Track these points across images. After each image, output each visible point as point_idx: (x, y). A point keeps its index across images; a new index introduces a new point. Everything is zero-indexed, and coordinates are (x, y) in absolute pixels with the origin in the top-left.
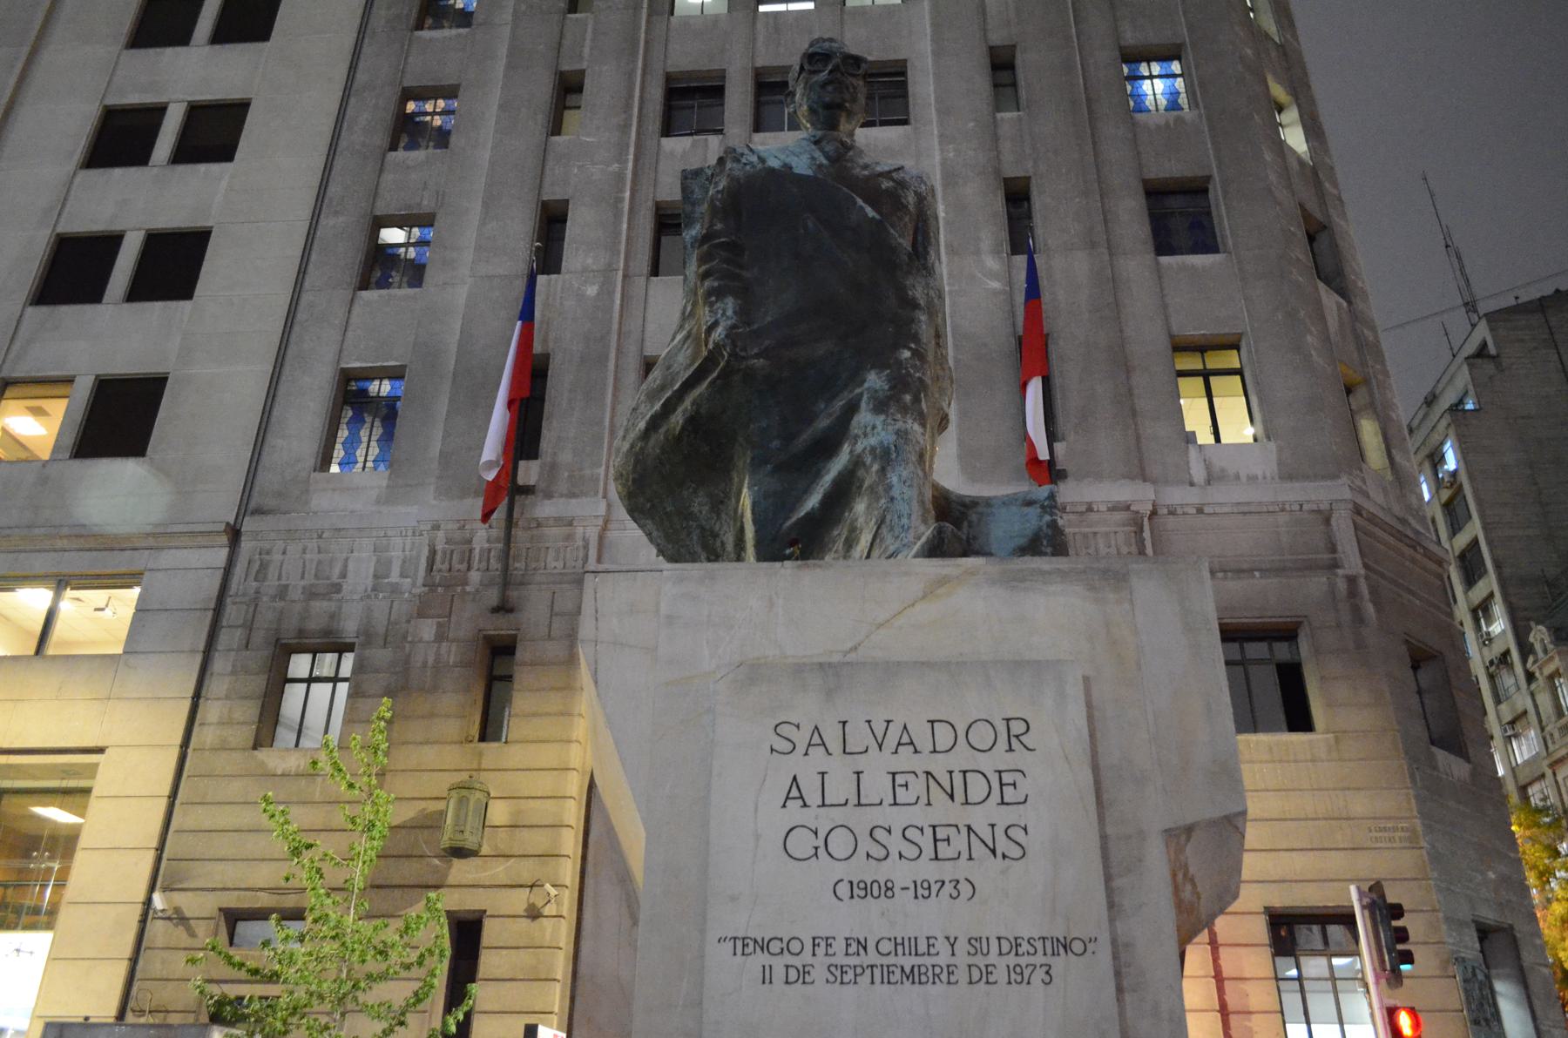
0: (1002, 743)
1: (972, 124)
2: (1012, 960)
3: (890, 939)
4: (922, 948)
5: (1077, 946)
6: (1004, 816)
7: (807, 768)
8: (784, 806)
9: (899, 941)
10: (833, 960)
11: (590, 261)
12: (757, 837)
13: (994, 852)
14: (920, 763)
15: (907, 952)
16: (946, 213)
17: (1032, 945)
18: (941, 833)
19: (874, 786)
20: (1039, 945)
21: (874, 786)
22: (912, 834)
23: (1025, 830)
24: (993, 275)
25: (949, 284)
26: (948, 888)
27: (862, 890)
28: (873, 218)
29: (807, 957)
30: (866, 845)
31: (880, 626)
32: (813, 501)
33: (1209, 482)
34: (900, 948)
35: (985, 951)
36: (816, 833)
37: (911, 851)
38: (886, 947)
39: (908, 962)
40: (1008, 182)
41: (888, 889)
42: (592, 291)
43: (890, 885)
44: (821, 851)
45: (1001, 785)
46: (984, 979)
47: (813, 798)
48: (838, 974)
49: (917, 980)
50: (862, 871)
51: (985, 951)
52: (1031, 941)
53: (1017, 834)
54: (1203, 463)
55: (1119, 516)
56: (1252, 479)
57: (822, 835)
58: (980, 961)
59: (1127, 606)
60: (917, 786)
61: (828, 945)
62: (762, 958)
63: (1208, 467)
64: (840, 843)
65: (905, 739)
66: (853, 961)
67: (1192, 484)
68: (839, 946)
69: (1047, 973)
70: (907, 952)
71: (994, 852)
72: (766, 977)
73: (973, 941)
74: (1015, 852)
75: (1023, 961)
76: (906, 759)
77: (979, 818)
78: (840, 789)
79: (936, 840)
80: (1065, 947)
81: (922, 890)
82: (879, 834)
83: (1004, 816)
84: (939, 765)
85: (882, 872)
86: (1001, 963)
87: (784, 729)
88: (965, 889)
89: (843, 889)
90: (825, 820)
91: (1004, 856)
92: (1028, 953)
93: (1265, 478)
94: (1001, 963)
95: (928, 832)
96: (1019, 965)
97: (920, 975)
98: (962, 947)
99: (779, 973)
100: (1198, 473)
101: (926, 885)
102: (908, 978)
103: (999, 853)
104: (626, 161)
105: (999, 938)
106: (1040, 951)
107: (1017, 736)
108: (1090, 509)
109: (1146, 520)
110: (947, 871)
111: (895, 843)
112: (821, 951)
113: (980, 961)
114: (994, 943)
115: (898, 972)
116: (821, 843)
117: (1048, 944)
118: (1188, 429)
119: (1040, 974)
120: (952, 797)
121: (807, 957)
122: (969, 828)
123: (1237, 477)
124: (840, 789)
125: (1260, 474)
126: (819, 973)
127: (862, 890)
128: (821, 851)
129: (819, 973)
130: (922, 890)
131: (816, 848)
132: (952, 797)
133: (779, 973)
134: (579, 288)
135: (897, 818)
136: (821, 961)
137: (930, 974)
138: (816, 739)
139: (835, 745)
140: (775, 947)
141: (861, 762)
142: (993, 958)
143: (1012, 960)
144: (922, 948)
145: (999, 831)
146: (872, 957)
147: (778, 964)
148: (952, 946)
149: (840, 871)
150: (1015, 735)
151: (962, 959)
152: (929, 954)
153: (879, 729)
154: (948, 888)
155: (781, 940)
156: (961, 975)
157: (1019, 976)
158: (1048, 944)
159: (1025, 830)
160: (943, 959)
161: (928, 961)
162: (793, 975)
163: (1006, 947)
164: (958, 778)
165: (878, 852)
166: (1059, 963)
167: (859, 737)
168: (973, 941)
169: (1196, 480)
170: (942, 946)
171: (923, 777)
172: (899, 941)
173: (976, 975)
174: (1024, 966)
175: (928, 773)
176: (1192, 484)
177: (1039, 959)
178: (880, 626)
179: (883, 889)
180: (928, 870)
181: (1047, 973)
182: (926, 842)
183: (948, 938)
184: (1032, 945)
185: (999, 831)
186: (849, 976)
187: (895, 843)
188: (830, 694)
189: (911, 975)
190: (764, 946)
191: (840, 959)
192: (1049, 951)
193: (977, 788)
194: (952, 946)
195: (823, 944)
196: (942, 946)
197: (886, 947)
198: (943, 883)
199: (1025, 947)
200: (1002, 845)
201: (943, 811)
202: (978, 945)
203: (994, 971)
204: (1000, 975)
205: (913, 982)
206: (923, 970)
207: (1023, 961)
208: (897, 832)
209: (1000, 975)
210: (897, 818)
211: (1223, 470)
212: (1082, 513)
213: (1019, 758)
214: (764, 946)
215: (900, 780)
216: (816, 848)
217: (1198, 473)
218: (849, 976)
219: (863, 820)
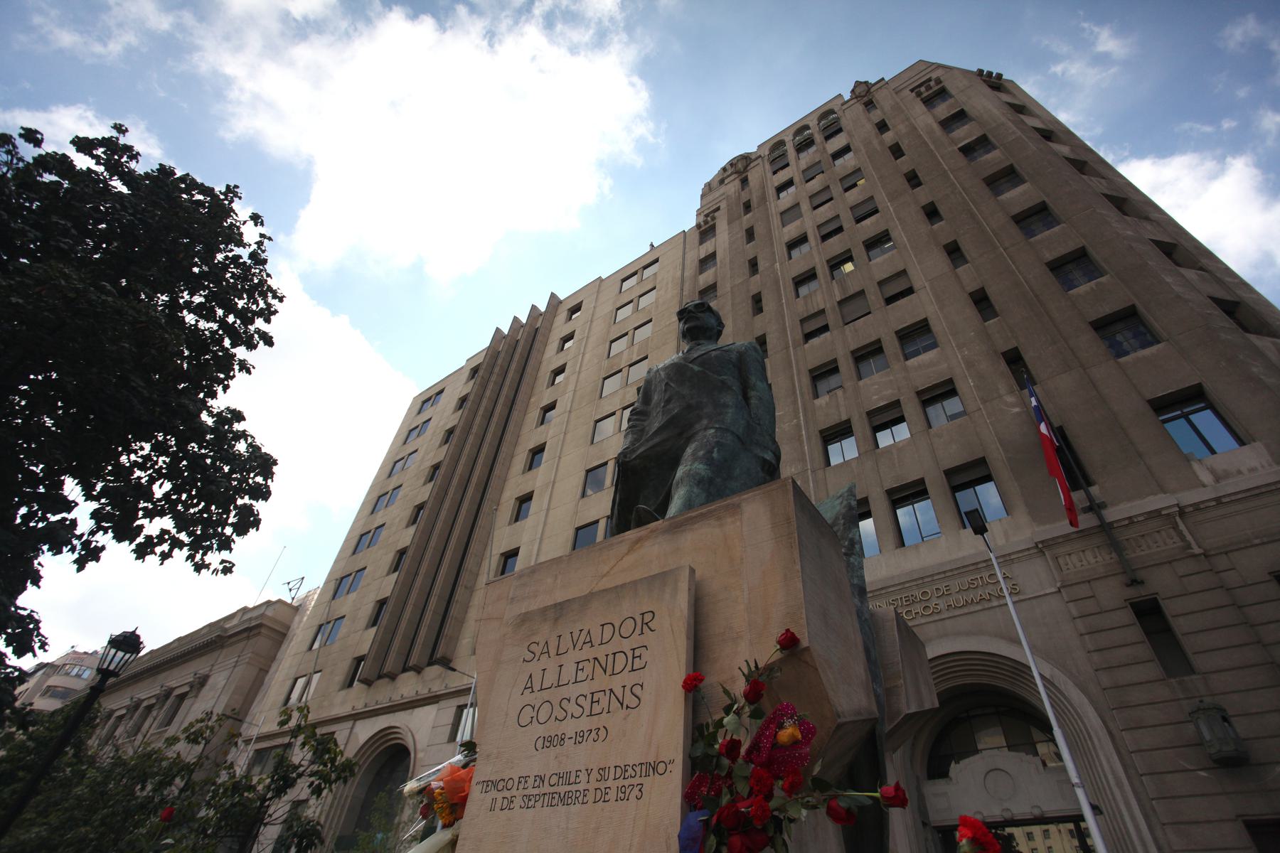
0: (638, 631)
1: (972, 334)
2: (621, 782)
3: (556, 774)
5: (661, 768)
6: (628, 679)
7: (535, 668)
8: (522, 694)
9: (561, 776)
10: (526, 792)
11: (793, 470)
12: (507, 715)
13: (622, 704)
15: (564, 783)
16: (974, 382)
17: (634, 771)
20: (638, 769)
23: (642, 686)
24: (1014, 406)
25: (989, 418)
26: (594, 733)
28: (699, 371)
29: (514, 792)
31: (605, 575)
34: (561, 779)
35: (606, 778)
36: (533, 708)
37: (578, 711)
38: (554, 780)
39: (562, 789)
40: (1004, 354)
41: (562, 739)
43: (563, 736)
44: (535, 719)
45: (634, 658)
46: (603, 799)
49: (566, 803)
50: (553, 729)
51: (606, 778)
52: (634, 767)
53: (637, 690)
56: (1253, 470)
57: (536, 709)
58: (602, 785)
59: (738, 523)
60: (588, 667)
61: (526, 782)
62: (494, 794)
63: (1212, 471)
65: (588, 640)
66: (536, 791)
67: (1204, 486)
68: (531, 781)
69: (640, 790)
70: (564, 783)
71: (622, 704)
73: (601, 771)
74: (633, 701)
75: (626, 783)
76: (587, 653)
77: (616, 683)
79: (592, 702)
80: (653, 769)
81: (580, 737)
84: (600, 652)
87: (533, 647)
88: (602, 732)
89: (540, 742)
91: (627, 707)
92: (631, 776)
93: (1263, 467)
95: (589, 697)
96: (624, 786)
97: (568, 798)
98: (595, 775)
99: (499, 805)
100: (1206, 477)
101: (581, 734)
102: (561, 800)
103: (625, 706)
104: (799, 417)
105: (616, 767)
106: (638, 773)
107: (647, 624)
110: (595, 722)
111: (572, 708)
112: (521, 786)
113: (602, 785)
114: (612, 770)
117: (644, 767)
119: (636, 791)
120: (605, 671)
121: (514, 792)
122: (611, 690)
123: (1239, 472)
124: (550, 679)
127: (549, 742)
128: (535, 719)
129: (518, 802)
130: (580, 737)
131: (532, 718)
132: (605, 671)
133: (499, 805)
135: (573, 691)
137: (573, 798)
138: (546, 650)
141: (563, 659)
143: (621, 782)
144: (572, 780)
145: (627, 690)
147: (499, 796)
148: (589, 775)
149: (540, 731)
150: (645, 623)
152: (576, 783)
154: (594, 733)
155: (504, 780)
156: (590, 797)
157: (623, 794)
158: (644, 767)
159: (642, 686)
160: (581, 787)
164: (611, 658)
165: (561, 715)
168: (601, 771)
170: (583, 777)
171: (592, 661)
172: (561, 776)
174: (627, 787)
179: (560, 739)
180: (584, 724)
181: (640, 790)
182: (587, 704)
183: (587, 770)
184: (634, 771)
185: (627, 690)
187: (572, 708)
188: (556, 620)
192: (644, 774)
194: (589, 775)
195: (523, 782)
196: (583, 777)
197: (554, 780)
198: (591, 730)
199: (630, 771)
201: (602, 681)
202: (603, 775)
203: (609, 792)
204: (612, 795)
205: (564, 805)
206: (571, 794)
207: (626, 783)
208: (573, 701)
209: (612, 795)
210: (573, 691)
213: (649, 637)
214: (495, 784)
215: (580, 667)
216: (532, 718)
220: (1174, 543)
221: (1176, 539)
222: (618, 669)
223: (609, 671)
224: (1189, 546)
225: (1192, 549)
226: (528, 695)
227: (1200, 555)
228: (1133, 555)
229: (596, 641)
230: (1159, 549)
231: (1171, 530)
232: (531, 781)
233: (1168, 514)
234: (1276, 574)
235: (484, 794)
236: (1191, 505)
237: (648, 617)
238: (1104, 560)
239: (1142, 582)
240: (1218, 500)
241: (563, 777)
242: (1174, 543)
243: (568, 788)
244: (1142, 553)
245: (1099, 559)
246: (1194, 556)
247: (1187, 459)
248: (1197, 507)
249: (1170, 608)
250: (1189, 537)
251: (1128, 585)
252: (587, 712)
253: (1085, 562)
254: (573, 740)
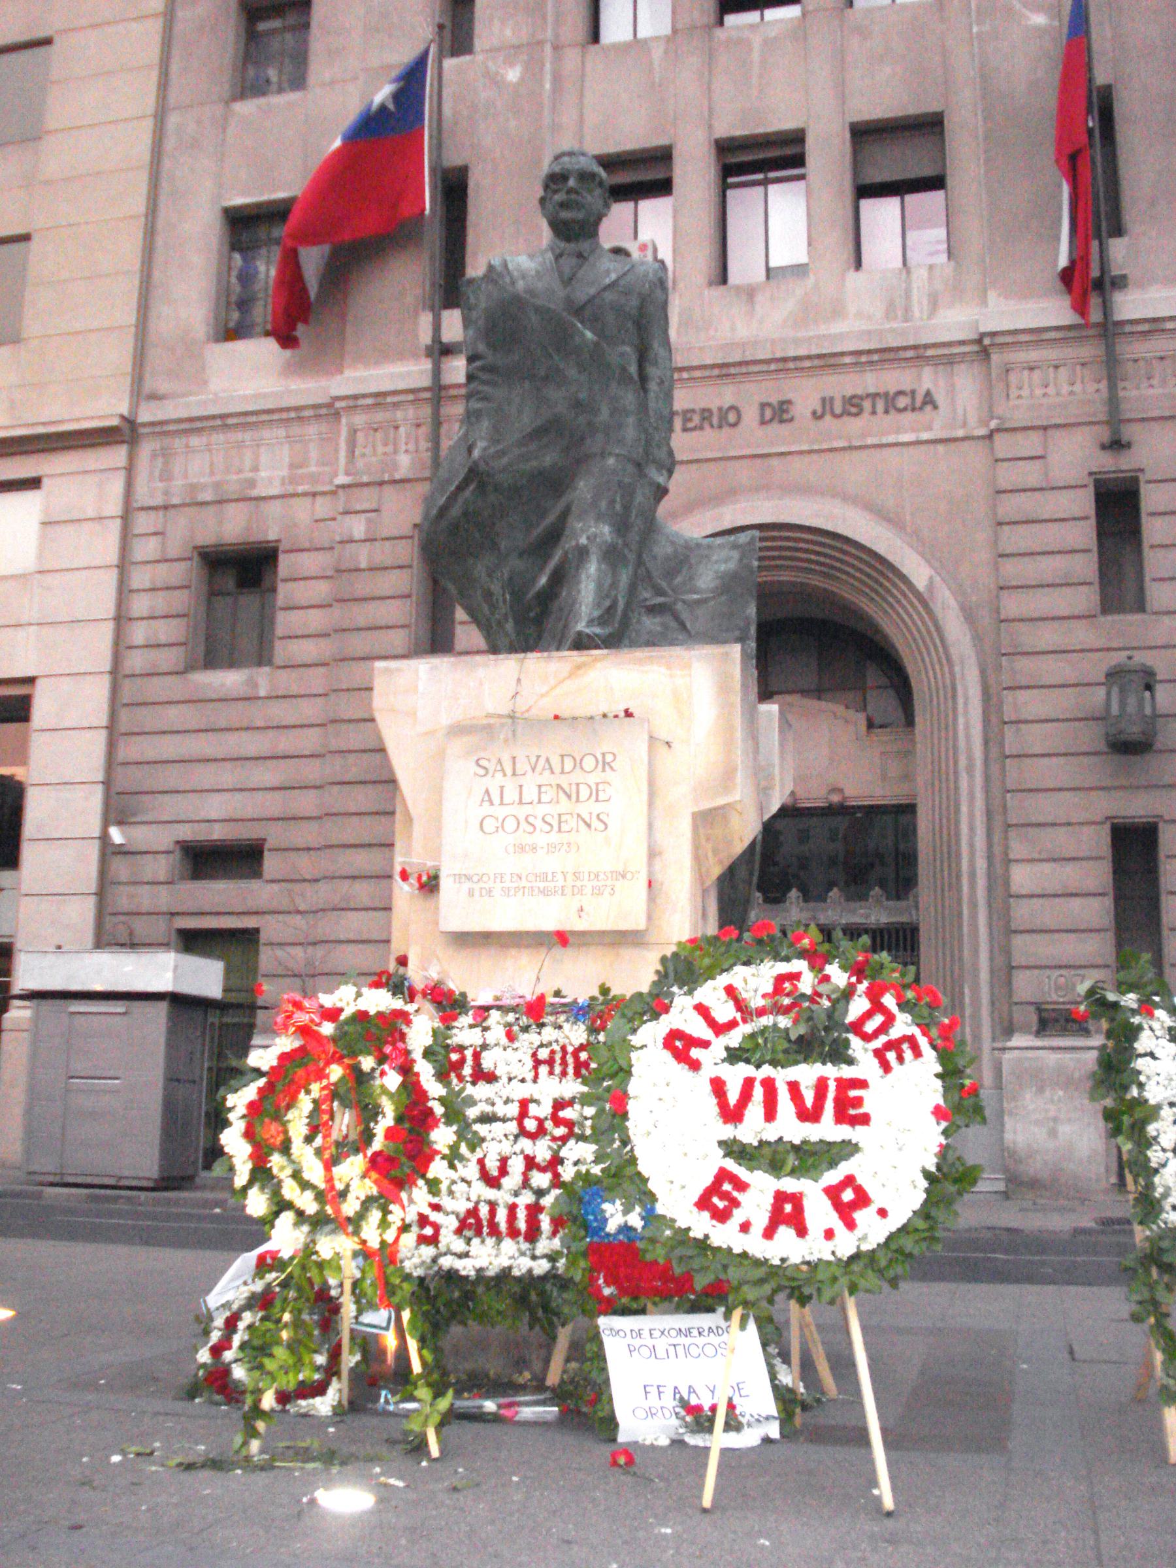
0: (600, 766)
2: (595, 883)
4: (550, 878)
5: (629, 876)
6: (597, 808)
7: (494, 783)
11: (508, 32)
14: (554, 780)
18: (563, 818)
19: (530, 793)
21: (530, 793)
22: (548, 819)
27: (521, 849)
29: (491, 884)
30: (523, 824)
31: (542, 696)
32: (543, 580)
37: (548, 828)
38: (531, 878)
39: (542, 885)
42: (513, 75)
47: (496, 800)
48: (506, 892)
57: (500, 820)
58: (579, 884)
62: (467, 885)
64: (510, 824)
72: (471, 893)
74: (602, 827)
75: (600, 884)
77: (584, 809)
78: (511, 795)
82: (531, 819)
83: (597, 808)
84: (564, 781)
85: (527, 840)
86: (589, 885)
87: (482, 762)
89: (511, 849)
90: (500, 812)
94: (589, 885)
95: (556, 817)
98: (570, 877)
111: (539, 823)
112: (498, 880)
115: (536, 890)
116: (499, 825)
119: (608, 890)
121: (491, 884)
122: (579, 815)
124: (511, 795)
126: (497, 892)
130: (552, 848)
133: (477, 893)
134: (497, 73)
135: (540, 810)
136: (499, 886)
138: (499, 768)
139: (509, 771)
140: (475, 879)
142: (586, 882)
143: (595, 883)
144: (550, 878)
146: (524, 883)
147: (477, 887)
151: (570, 882)
153: (533, 760)
154: (565, 847)
156: (568, 891)
157: (597, 892)
160: (561, 883)
161: (552, 885)
162: (484, 892)
163: (592, 876)
164: (574, 787)
166: (619, 885)
167: (522, 766)
170: (560, 877)
173: (576, 891)
175: (559, 786)
177: (609, 882)
178: (542, 696)
182: (555, 824)
186: (512, 892)
187: (539, 823)
189: (544, 892)
190: (469, 878)
191: (508, 884)
193: (584, 792)
199: (602, 877)
200: (595, 823)
201: (565, 805)
204: (588, 890)
209: (588, 890)
213: (609, 775)
214: (469, 878)
215: (543, 789)
218: (512, 892)
219: (522, 812)
222: (582, 798)
223: (574, 796)
226: (486, 809)
229: (557, 770)
232: (507, 878)
235: (458, 885)
237: (609, 758)
238: (1084, 391)
239: (1128, 445)
241: (544, 877)
243: (546, 884)
244: (1152, 391)
245: (1077, 388)
249: (1151, 498)
251: (1104, 447)
252: (556, 828)
253: (1051, 390)
254: (545, 850)
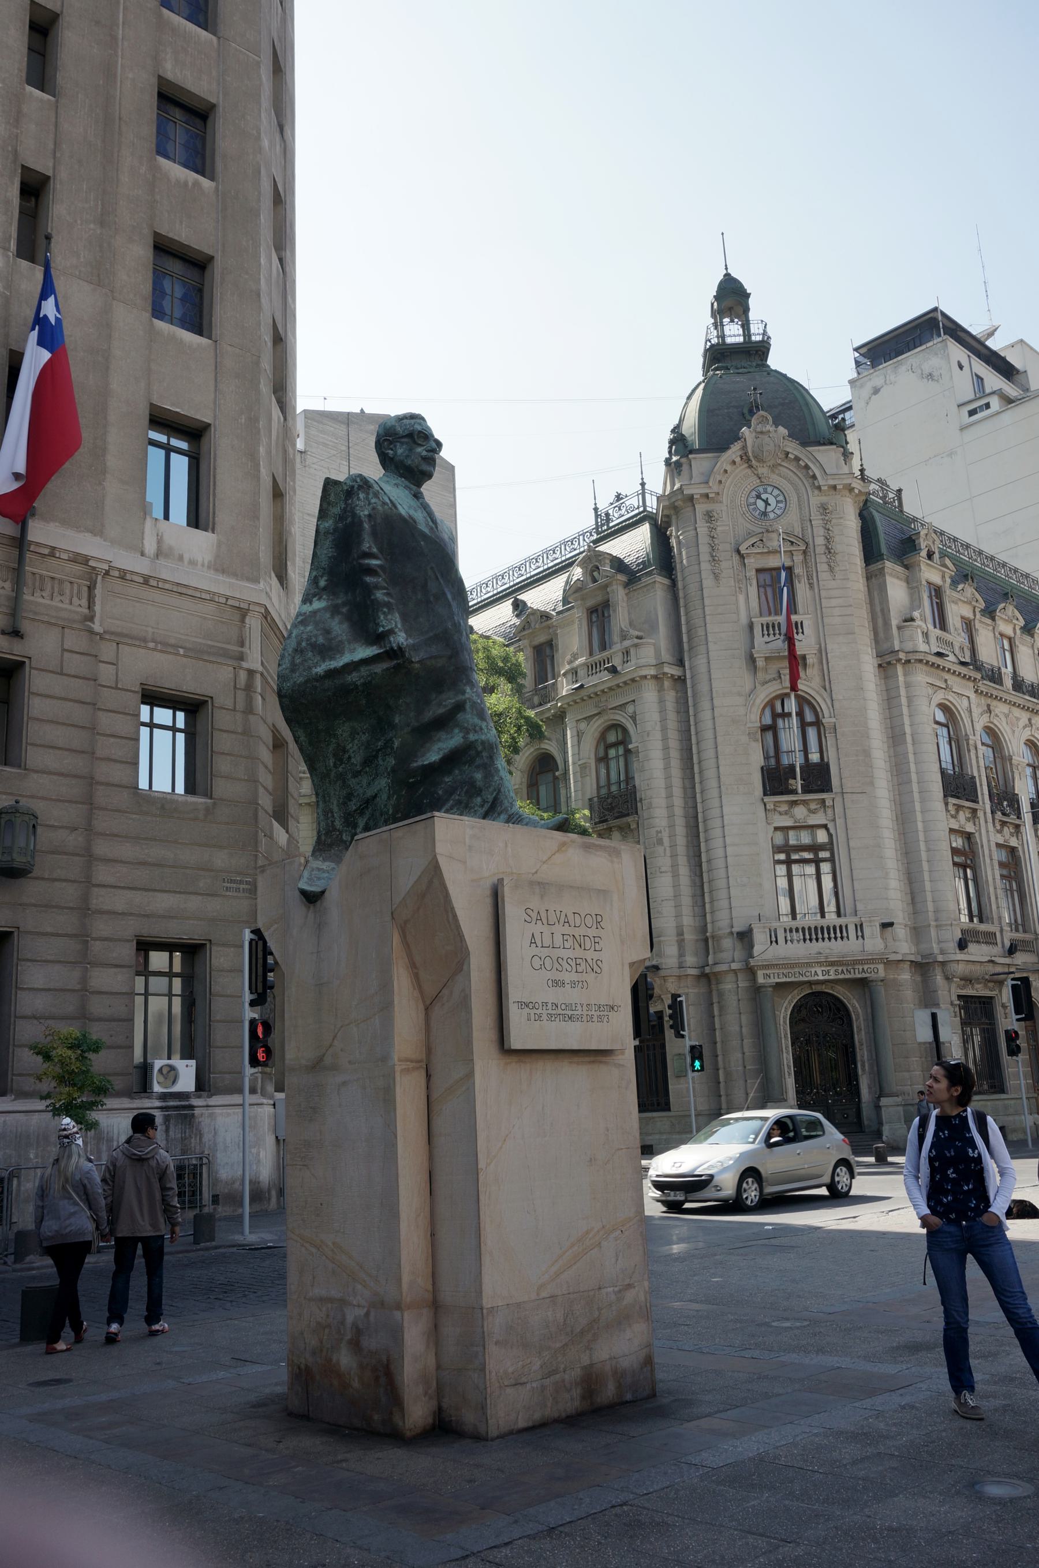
33: (157, 556)
54: (155, 538)
55: (77, 568)
56: (192, 563)
63: (160, 541)
67: (143, 554)
100: (150, 546)
108: (52, 555)
109: (100, 578)
118: (148, 499)
123: (181, 558)
125: (200, 560)
169: (147, 551)
176: (143, 554)
211: (171, 548)
212: (44, 555)
217: (150, 546)
220: (80, 605)
221: (84, 602)
224: (91, 619)
225: (94, 623)
227: (97, 634)
228: (31, 598)
230: (60, 605)
231: (86, 589)
233: (94, 568)
234: (146, 687)
236: (119, 570)
240: (146, 580)
242: (80, 605)
246: (91, 632)
247: (145, 509)
248: (123, 574)
250: (97, 608)
